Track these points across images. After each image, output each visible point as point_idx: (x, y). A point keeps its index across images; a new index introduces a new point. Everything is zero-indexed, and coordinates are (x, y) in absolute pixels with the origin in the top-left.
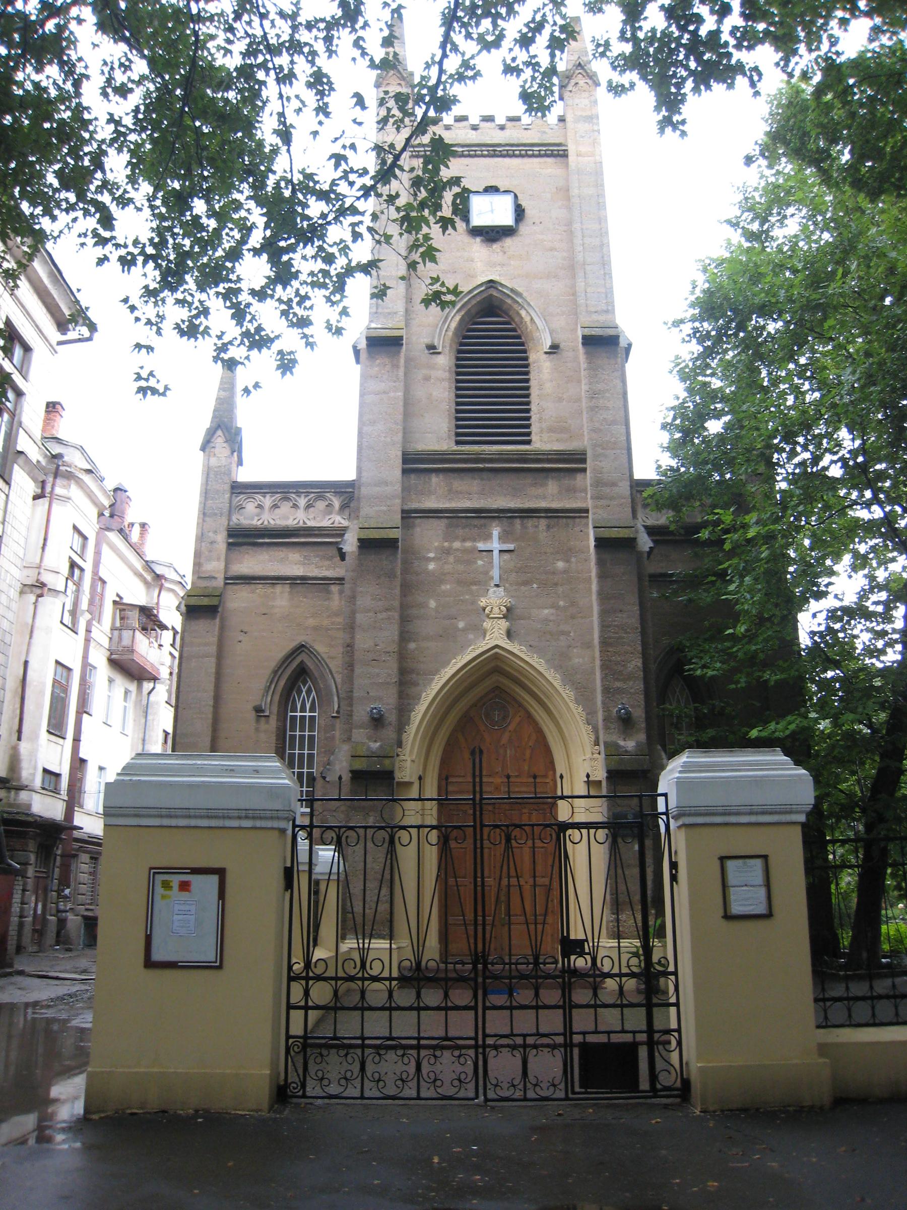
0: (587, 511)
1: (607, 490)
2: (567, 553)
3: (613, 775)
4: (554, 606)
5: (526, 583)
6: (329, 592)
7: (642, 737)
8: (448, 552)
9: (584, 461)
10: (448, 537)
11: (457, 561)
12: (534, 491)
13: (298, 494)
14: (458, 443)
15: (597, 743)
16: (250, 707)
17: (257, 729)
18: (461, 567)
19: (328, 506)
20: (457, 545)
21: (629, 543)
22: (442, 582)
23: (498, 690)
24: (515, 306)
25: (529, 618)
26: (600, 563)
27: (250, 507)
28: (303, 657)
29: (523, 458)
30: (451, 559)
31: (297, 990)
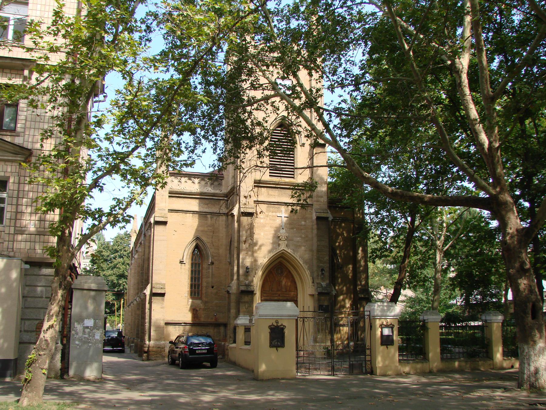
0: (312, 205)
3: (320, 294)
4: (301, 237)
5: (292, 228)
6: (207, 217)
7: (328, 282)
11: (270, 219)
13: (195, 178)
14: (270, 176)
15: (313, 283)
17: (181, 268)
18: (272, 222)
19: (206, 183)
20: (270, 214)
21: (327, 218)
23: (281, 264)
25: (293, 240)
26: (317, 224)
30: (268, 218)
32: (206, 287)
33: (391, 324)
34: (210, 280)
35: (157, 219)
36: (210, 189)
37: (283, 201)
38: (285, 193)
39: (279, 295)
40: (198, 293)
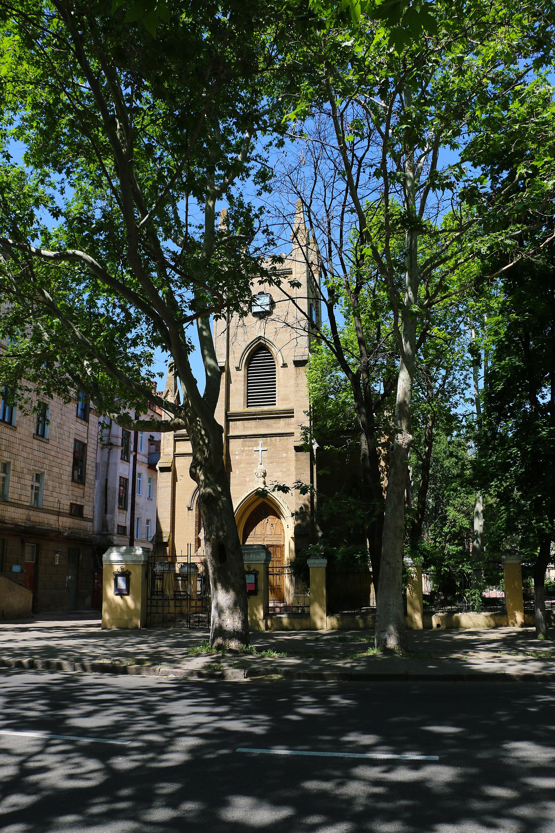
5: (271, 463)
8: (243, 451)
9: (293, 413)
10: (244, 445)
11: (247, 455)
16: (185, 506)
18: (248, 457)
20: (246, 449)
22: (241, 463)
24: (270, 347)
26: (296, 456)
30: (244, 454)
31: (149, 602)
33: (254, 570)
37: (260, 433)
38: (262, 424)
39: (264, 540)
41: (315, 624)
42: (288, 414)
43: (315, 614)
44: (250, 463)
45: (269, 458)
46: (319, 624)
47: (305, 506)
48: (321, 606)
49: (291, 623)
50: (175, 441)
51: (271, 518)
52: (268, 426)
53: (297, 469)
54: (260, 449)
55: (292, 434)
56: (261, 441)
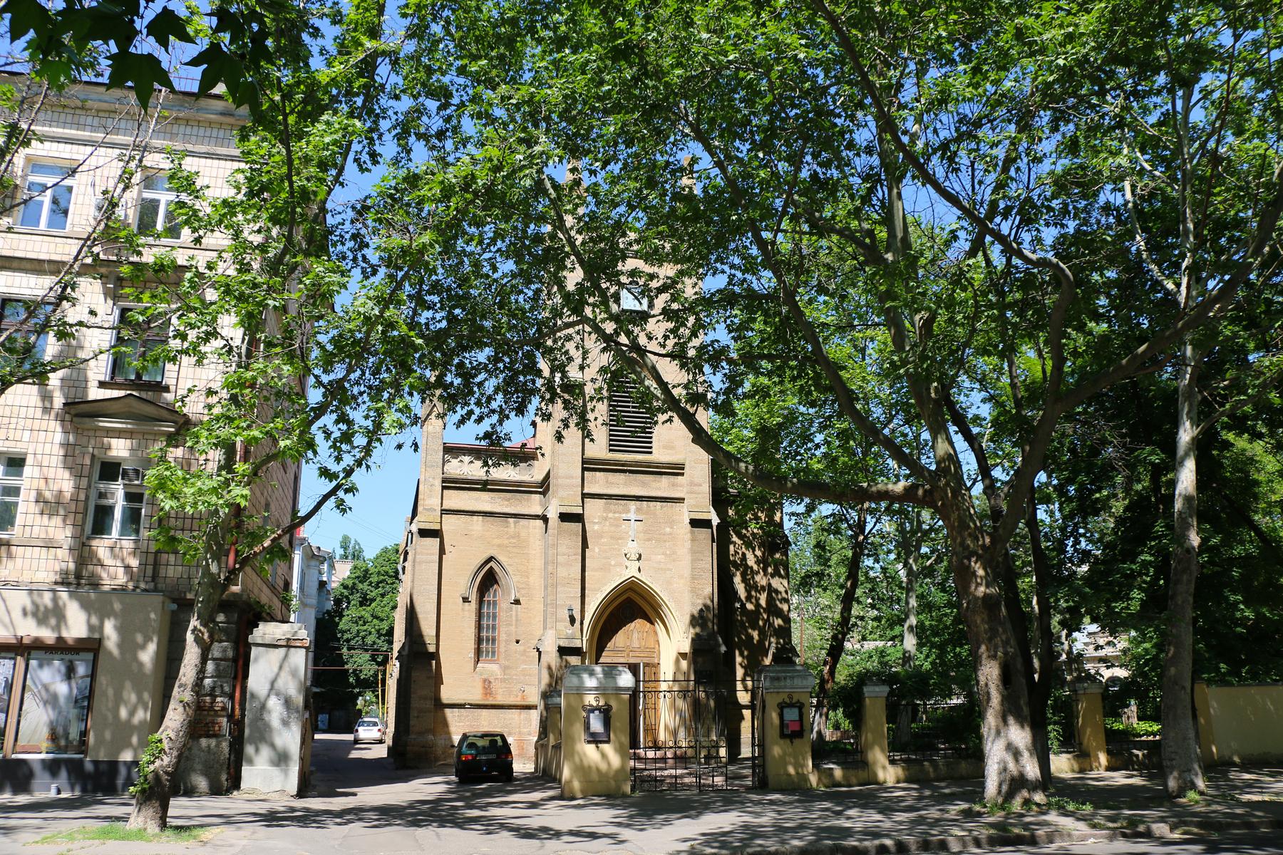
1: (696, 488)
2: (671, 523)
5: (649, 540)
8: (606, 519)
10: (606, 510)
11: (611, 525)
12: (654, 485)
18: (613, 529)
20: (611, 515)
26: (692, 533)
27: (455, 462)
28: (492, 564)
29: (649, 464)
32: (506, 641)
34: (513, 628)
35: (423, 526)
36: (513, 473)
40: (493, 653)
41: (875, 775)
42: (676, 470)
43: (875, 763)
44: (617, 538)
45: (645, 532)
46: (881, 775)
47: (706, 606)
48: (883, 750)
49: (844, 776)
50: (444, 488)
51: (638, 625)
52: (644, 484)
53: (693, 552)
54: (632, 516)
55: (681, 500)
56: (633, 505)
